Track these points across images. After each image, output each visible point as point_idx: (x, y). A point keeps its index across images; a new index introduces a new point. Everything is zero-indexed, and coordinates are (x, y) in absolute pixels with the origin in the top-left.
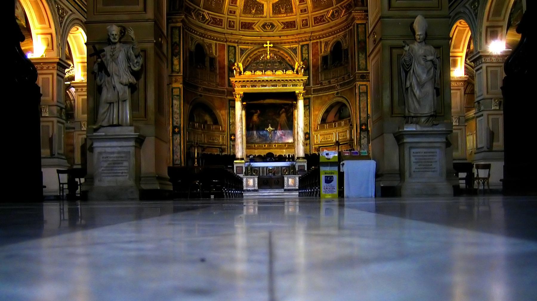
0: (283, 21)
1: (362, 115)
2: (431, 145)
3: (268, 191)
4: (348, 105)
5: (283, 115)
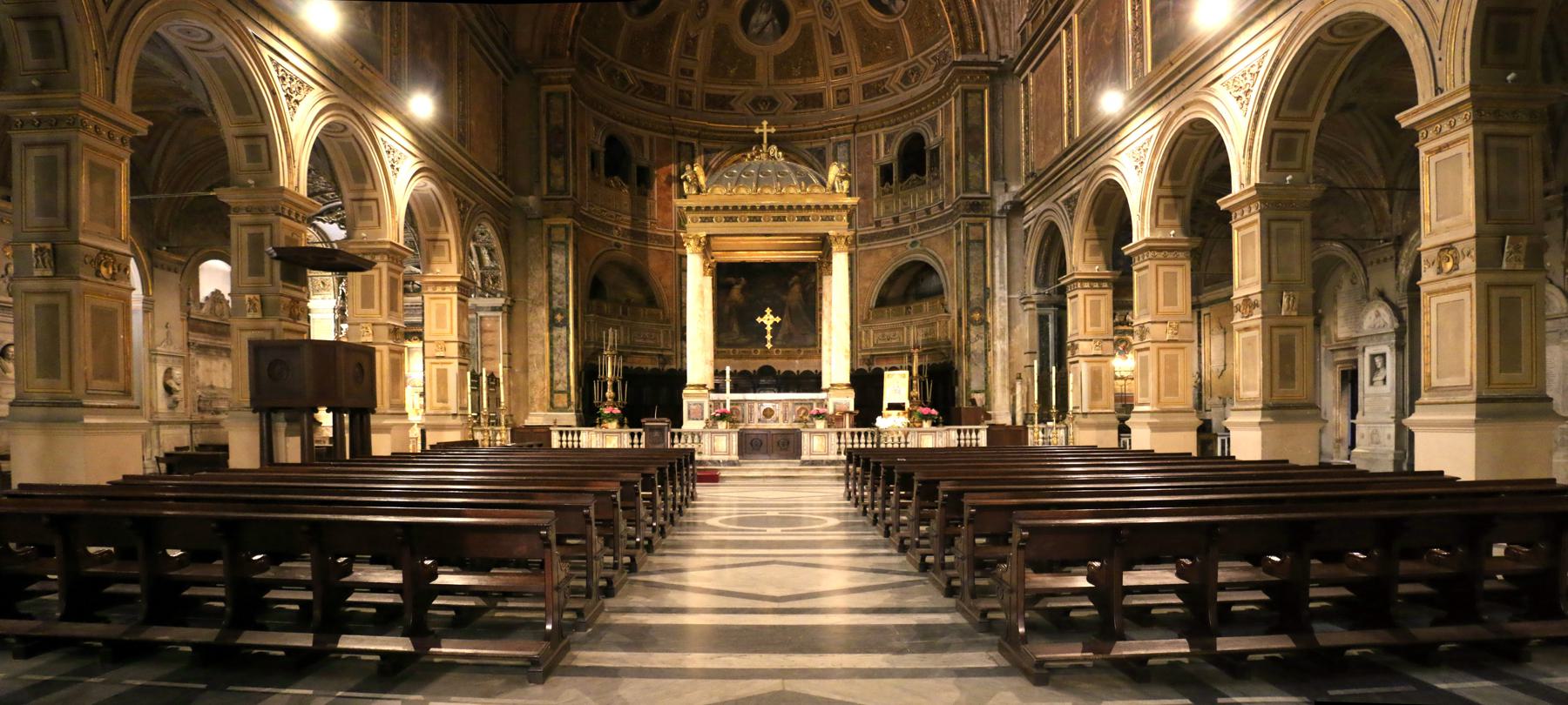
0: (797, 94)
1: (972, 288)
3: (763, 466)
4: (938, 270)
5: (796, 288)
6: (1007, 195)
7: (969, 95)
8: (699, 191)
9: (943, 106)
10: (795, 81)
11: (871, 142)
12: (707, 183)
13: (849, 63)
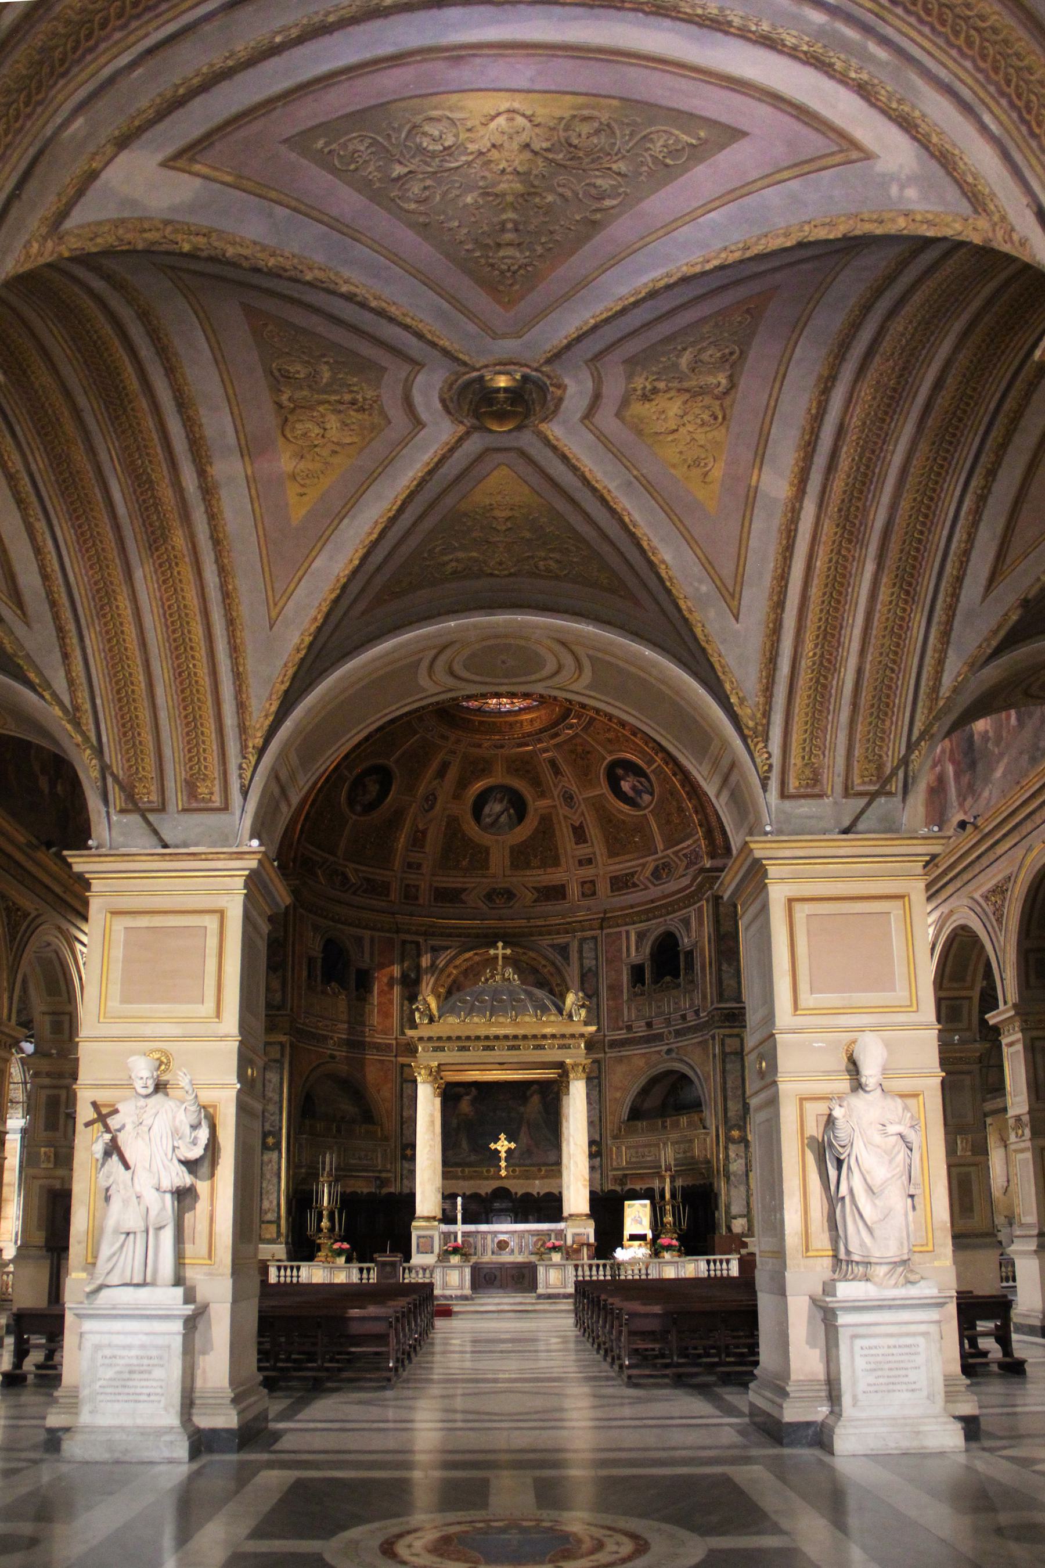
2: (905, 1329)
8: (431, 1020)
11: (620, 939)
12: (439, 1008)
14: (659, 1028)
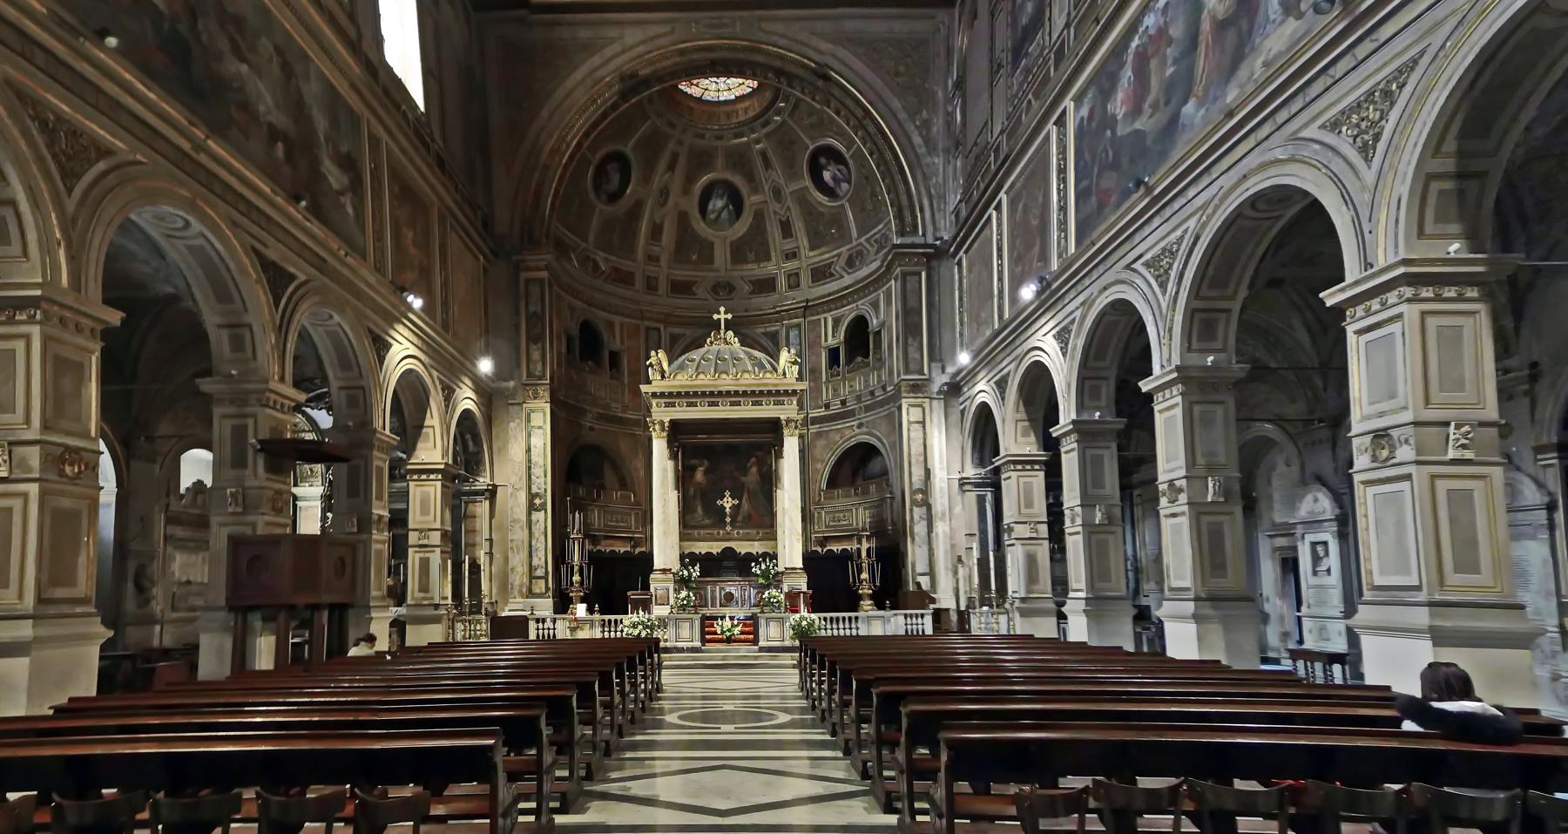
0: (752, 278)
6: (944, 376)
7: (908, 278)
8: (663, 377)
9: (884, 288)
10: (750, 266)
11: (820, 326)
13: (798, 247)
14: (851, 405)
